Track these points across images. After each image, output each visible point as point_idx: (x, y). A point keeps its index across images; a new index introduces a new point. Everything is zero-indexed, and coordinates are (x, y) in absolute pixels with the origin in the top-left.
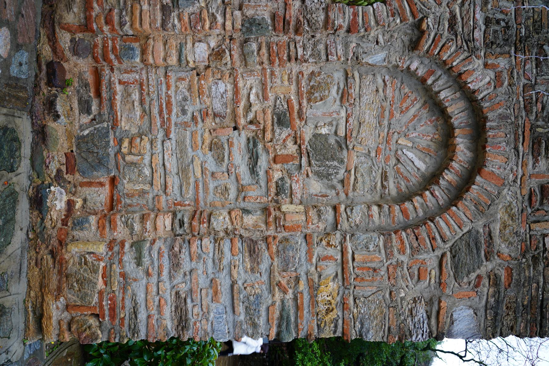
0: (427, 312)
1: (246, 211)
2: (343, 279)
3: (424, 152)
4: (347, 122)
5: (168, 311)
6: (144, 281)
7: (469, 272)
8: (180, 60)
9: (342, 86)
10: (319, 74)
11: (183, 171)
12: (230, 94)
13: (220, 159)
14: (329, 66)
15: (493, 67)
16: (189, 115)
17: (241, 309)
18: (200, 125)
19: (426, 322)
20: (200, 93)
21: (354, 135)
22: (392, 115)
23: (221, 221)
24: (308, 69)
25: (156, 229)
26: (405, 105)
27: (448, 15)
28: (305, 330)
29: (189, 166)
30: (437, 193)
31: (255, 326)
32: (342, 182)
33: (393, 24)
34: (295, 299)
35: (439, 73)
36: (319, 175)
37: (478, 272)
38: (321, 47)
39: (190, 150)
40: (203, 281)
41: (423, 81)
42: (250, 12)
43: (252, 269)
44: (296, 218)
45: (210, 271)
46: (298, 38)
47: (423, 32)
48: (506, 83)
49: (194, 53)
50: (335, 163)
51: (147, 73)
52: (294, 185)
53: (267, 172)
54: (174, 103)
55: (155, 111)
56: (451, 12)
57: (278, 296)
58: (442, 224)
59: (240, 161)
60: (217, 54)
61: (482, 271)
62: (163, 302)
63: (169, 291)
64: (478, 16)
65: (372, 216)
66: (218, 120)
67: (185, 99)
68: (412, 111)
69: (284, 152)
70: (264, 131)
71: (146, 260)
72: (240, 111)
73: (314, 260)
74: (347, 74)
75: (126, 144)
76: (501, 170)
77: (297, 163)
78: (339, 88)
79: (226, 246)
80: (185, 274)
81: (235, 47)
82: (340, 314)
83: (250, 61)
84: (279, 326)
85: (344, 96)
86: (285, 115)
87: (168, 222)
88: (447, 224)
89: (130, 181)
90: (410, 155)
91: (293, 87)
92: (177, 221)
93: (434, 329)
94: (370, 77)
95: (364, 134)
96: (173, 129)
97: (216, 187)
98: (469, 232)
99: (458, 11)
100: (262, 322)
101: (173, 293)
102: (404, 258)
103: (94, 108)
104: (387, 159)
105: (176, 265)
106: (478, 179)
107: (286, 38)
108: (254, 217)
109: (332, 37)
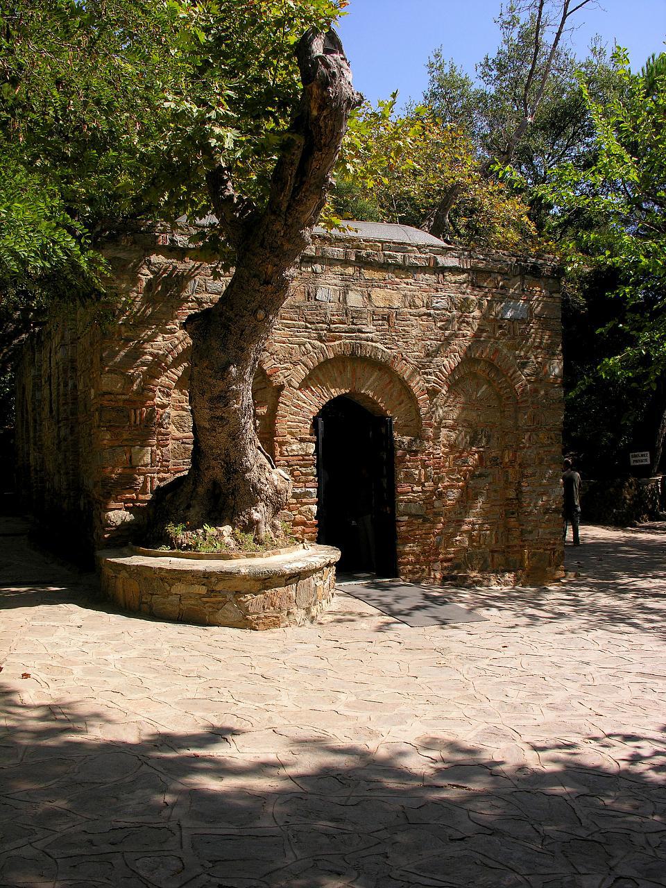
3: (479, 386)
87: (512, 520)
92: (511, 516)
102: (530, 400)
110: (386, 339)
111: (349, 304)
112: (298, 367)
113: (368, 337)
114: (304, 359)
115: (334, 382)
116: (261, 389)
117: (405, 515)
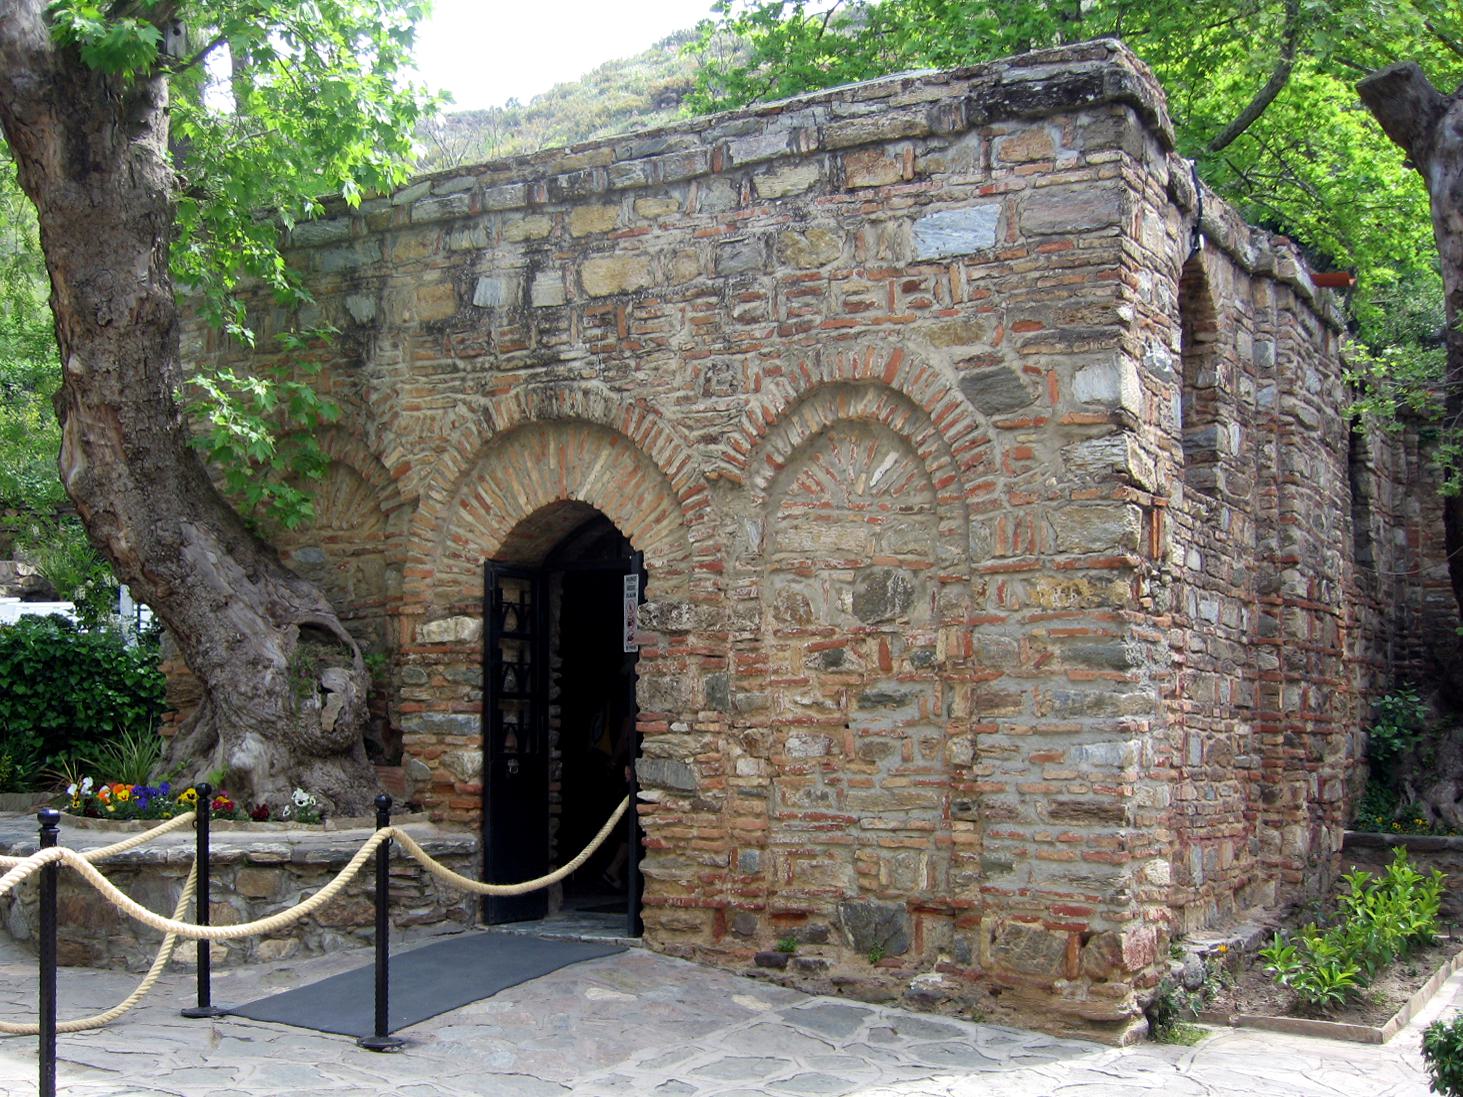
0: (1082, 441)
1: (949, 710)
2: (1030, 570)
3: (874, 455)
4: (835, 568)
5: (1080, 830)
6: (1034, 862)
7: (1021, 387)
8: (759, 796)
9: (790, 577)
10: (776, 608)
11: (902, 803)
12: (802, 731)
13: (885, 749)
14: (767, 594)
15: (758, 381)
16: (827, 789)
17: (1072, 723)
18: (840, 775)
19: (1095, 442)
20: (800, 773)
21: (853, 557)
22: (827, 505)
23: (960, 750)
24: (770, 623)
25: (971, 844)
26: (814, 487)
27: (702, 447)
28: (1104, 625)
29: (893, 795)
30: (920, 438)
31: (1099, 703)
32: (915, 573)
33: (713, 516)
34: (1062, 641)
35: (769, 448)
36: (904, 609)
37: (1019, 373)
38: (741, 607)
39: (873, 791)
40: (1033, 778)
41: (779, 468)
42: (701, 699)
43: (1016, 704)
44: (953, 640)
45: (1020, 765)
46: (731, 638)
47: (720, 476)
48: (777, 362)
49: (749, 776)
50: (890, 583)
51: (776, 845)
52: (919, 643)
53: (901, 681)
54: (814, 810)
55: (823, 836)
56: (699, 442)
57: (1055, 666)
58: (952, 432)
59: (885, 721)
60: (750, 745)
61: (1016, 365)
62: (1062, 838)
63: (1049, 828)
64: (702, 407)
65: (950, 530)
66: (835, 750)
67: (808, 794)
68: (822, 476)
69: (875, 657)
70: (849, 685)
71: (1003, 856)
72: (821, 717)
73: (1003, 614)
74: (775, 571)
75: (865, 882)
76: (884, 353)
77: (889, 639)
78: (794, 581)
79: (985, 741)
80: (1023, 802)
81: (740, 723)
82: (1080, 574)
83: (759, 702)
84: (1100, 665)
85: (803, 572)
86: (827, 655)
87: (961, 826)
88: (952, 424)
89: (915, 881)
90: (877, 476)
91: (793, 643)
92: (960, 814)
93: (1105, 428)
94: (779, 538)
95: (852, 543)
96: (847, 815)
97: (923, 756)
98: (963, 390)
99: (696, 433)
100: (1093, 692)
101: (1052, 821)
103: (821, 923)
104: (883, 508)
105: (1011, 814)
106: (895, 385)
107: (731, 654)
108: (957, 700)
109: (730, 593)
110: (609, 370)
111: (536, 304)
112: (446, 457)
113: (570, 370)
114: (455, 436)
115: (526, 481)
116: (393, 509)
117: (652, 786)
